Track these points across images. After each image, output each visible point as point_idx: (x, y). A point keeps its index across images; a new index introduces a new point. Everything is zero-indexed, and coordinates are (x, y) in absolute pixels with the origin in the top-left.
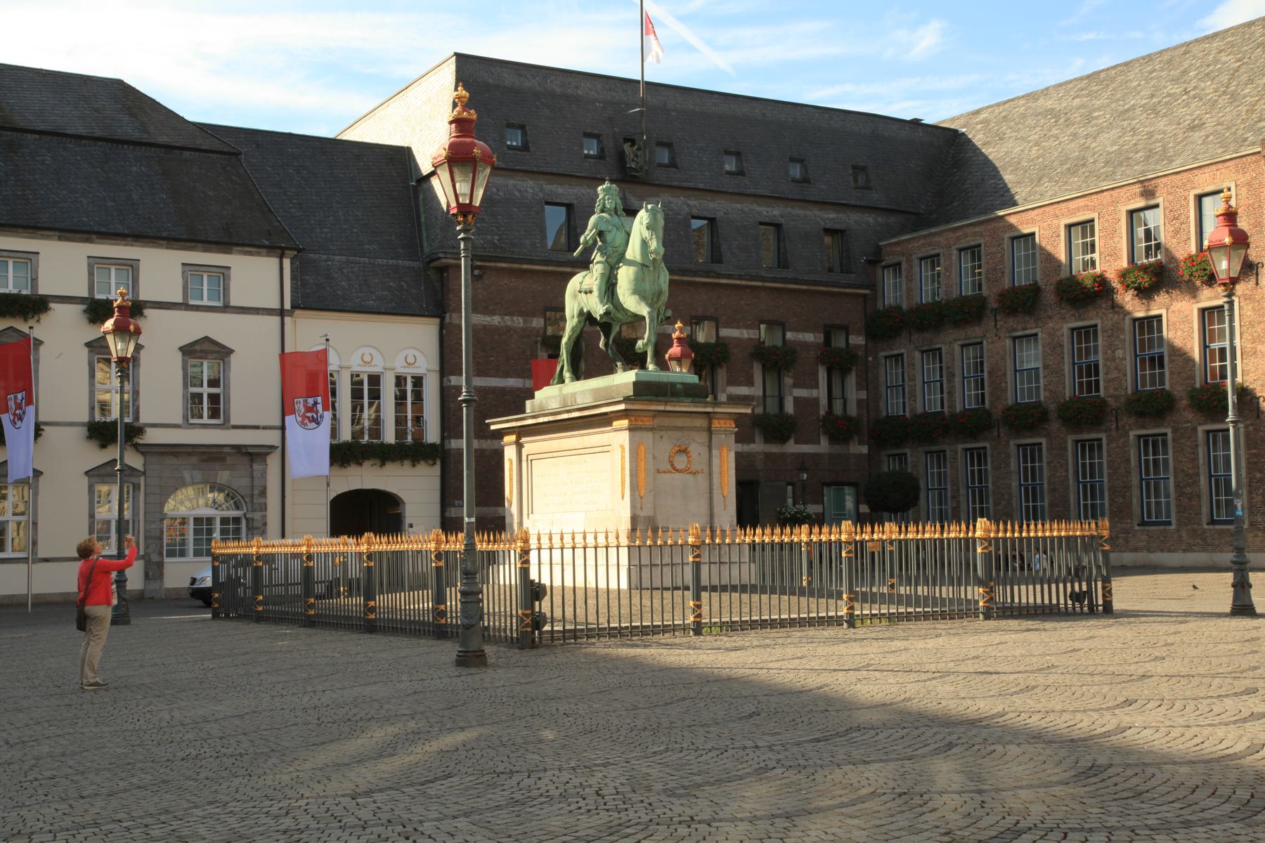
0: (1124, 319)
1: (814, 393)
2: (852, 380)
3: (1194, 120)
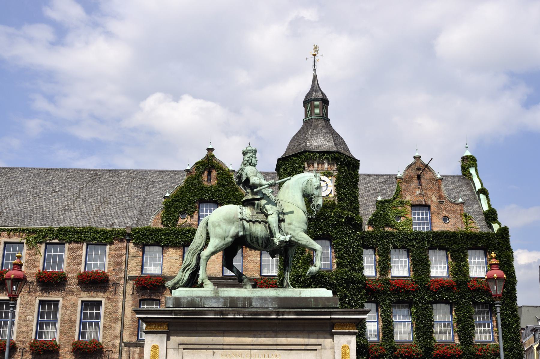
0: (35, 299)
3: (65, 206)
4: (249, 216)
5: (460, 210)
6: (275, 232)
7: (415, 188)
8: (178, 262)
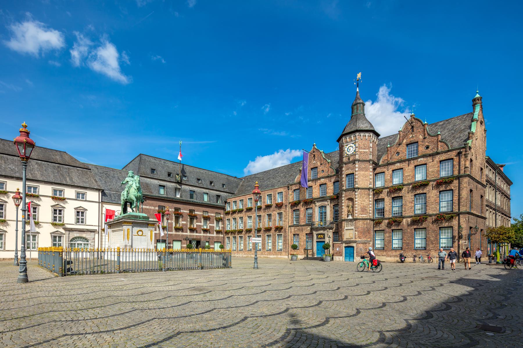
1: (213, 225)
2: (220, 223)
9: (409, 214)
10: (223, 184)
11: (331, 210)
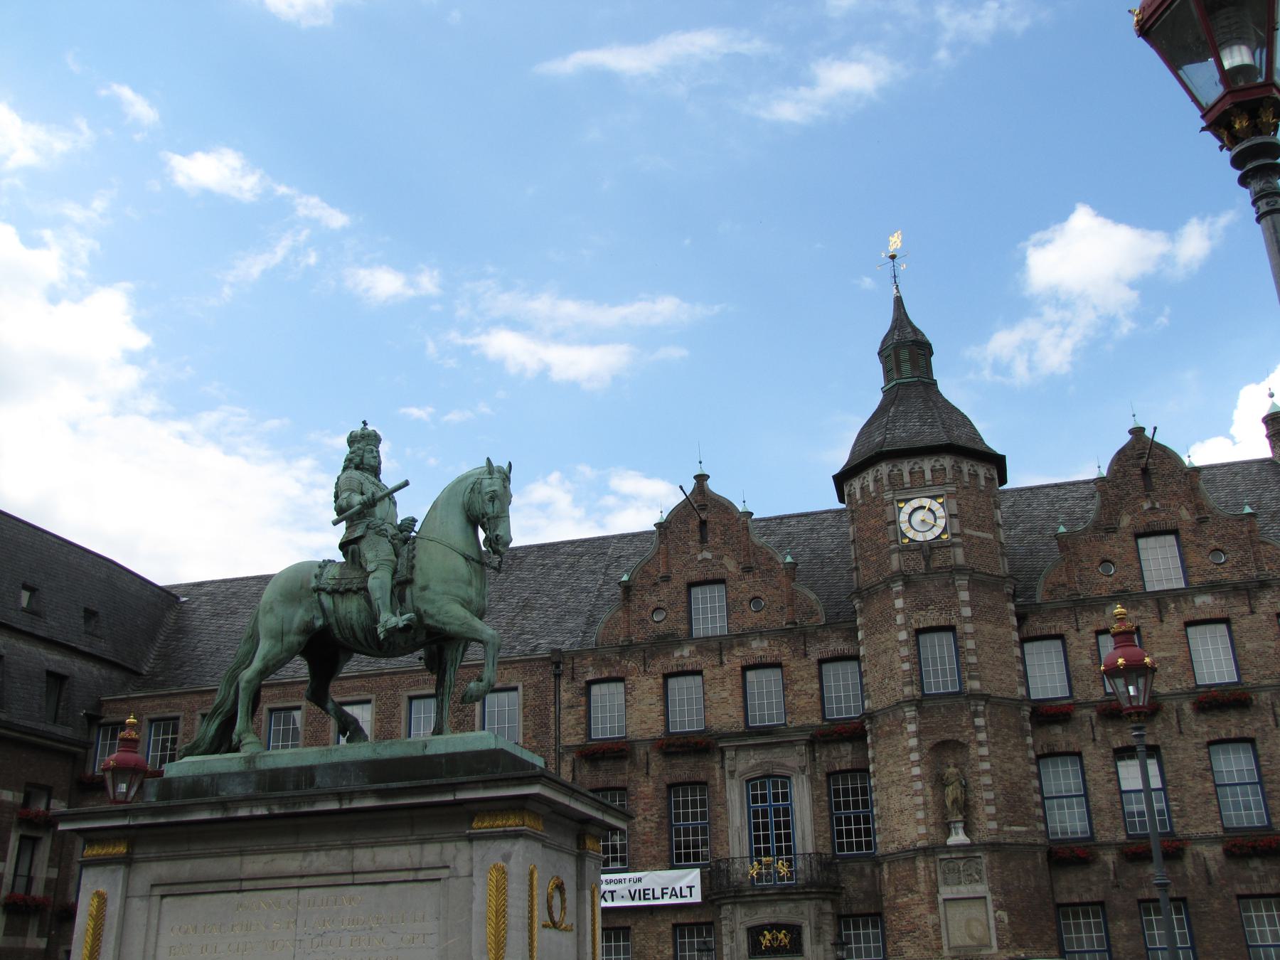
4: (333, 582)
5: (1250, 532)
6: (379, 610)
7: (1139, 497)
8: (655, 710)
9: (1203, 829)
10: (86, 610)
11: (815, 801)
